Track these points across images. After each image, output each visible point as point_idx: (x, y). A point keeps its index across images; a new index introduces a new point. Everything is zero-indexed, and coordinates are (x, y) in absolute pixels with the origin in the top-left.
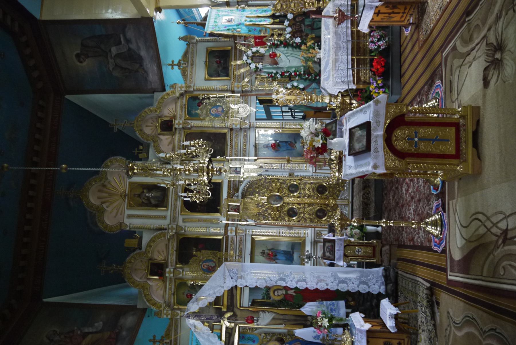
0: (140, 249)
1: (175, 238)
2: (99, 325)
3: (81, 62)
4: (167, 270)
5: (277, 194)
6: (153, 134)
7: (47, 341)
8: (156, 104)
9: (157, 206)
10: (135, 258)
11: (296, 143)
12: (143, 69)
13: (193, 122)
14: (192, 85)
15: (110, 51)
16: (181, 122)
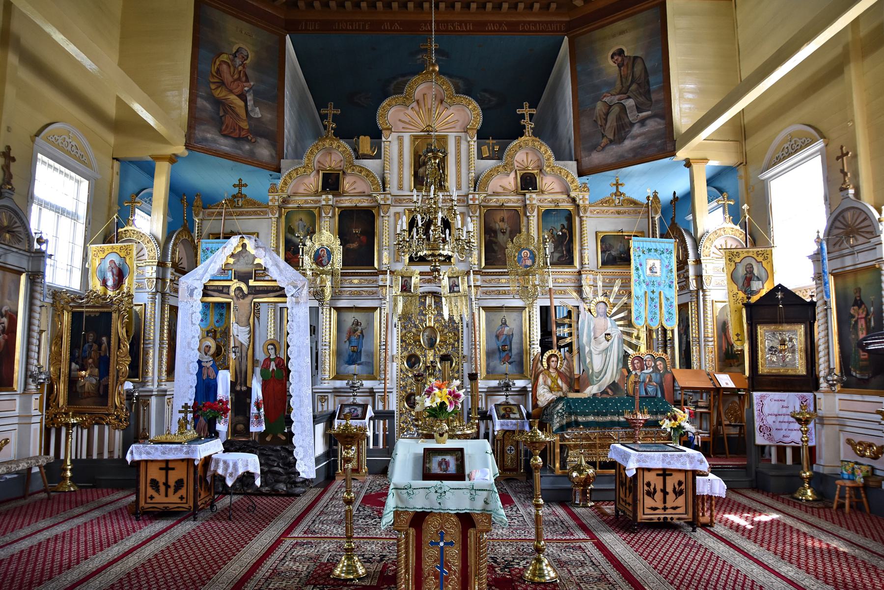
0: (357, 158)
1: (373, 204)
2: (257, 113)
3: (612, 57)
4: (330, 197)
5: (438, 340)
6: (516, 164)
7: (234, 51)
8: (560, 164)
9: (416, 175)
10: (344, 152)
11: (510, 363)
12: (607, 145)
13: (536, 218)
14: (588, 214)
15: (629, 97)
16: (534, 202)
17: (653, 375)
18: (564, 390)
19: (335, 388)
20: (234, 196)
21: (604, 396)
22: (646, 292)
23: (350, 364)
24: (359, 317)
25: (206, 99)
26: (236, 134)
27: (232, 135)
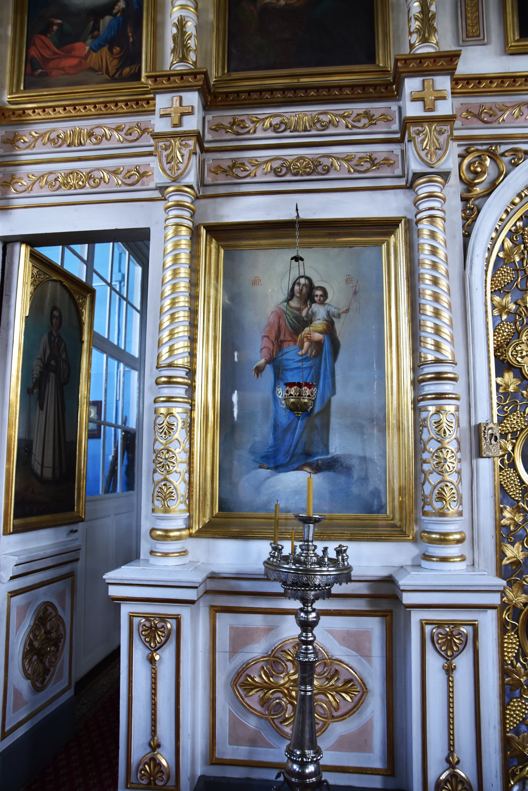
19: (213, 577)
23: (279, 467)
24: (322, 265)
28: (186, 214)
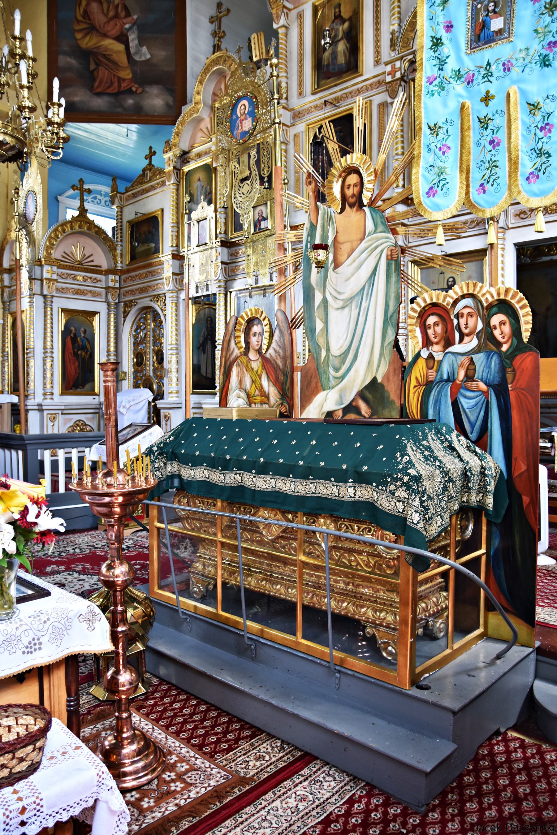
17: (479, 359)
18: (272, 400)
20: (144, 170)
21: (352, 416)
22: (463, 106)
25: (69, 54)
26: (114, 89)
27: (110, 91)
28: (223, 289)
